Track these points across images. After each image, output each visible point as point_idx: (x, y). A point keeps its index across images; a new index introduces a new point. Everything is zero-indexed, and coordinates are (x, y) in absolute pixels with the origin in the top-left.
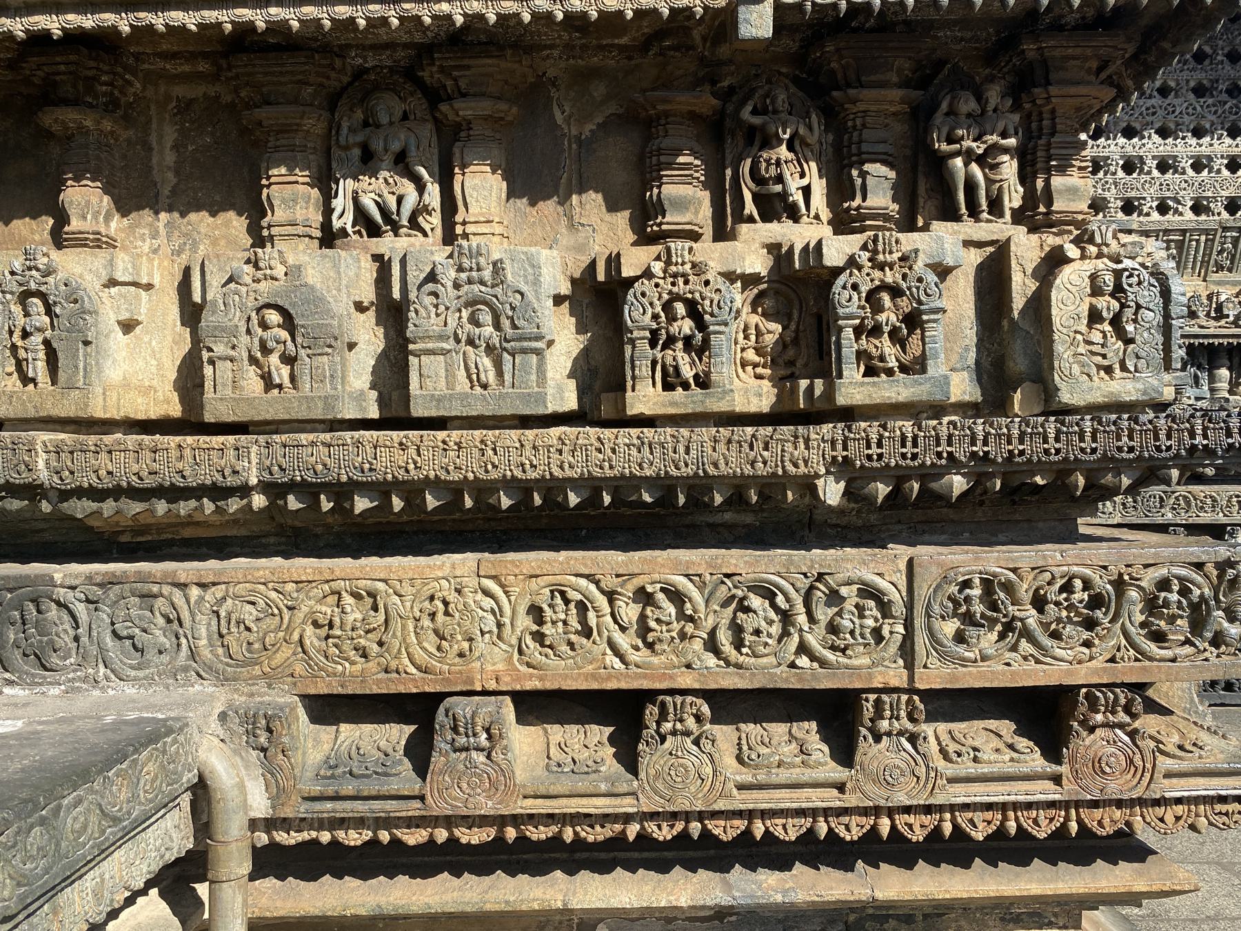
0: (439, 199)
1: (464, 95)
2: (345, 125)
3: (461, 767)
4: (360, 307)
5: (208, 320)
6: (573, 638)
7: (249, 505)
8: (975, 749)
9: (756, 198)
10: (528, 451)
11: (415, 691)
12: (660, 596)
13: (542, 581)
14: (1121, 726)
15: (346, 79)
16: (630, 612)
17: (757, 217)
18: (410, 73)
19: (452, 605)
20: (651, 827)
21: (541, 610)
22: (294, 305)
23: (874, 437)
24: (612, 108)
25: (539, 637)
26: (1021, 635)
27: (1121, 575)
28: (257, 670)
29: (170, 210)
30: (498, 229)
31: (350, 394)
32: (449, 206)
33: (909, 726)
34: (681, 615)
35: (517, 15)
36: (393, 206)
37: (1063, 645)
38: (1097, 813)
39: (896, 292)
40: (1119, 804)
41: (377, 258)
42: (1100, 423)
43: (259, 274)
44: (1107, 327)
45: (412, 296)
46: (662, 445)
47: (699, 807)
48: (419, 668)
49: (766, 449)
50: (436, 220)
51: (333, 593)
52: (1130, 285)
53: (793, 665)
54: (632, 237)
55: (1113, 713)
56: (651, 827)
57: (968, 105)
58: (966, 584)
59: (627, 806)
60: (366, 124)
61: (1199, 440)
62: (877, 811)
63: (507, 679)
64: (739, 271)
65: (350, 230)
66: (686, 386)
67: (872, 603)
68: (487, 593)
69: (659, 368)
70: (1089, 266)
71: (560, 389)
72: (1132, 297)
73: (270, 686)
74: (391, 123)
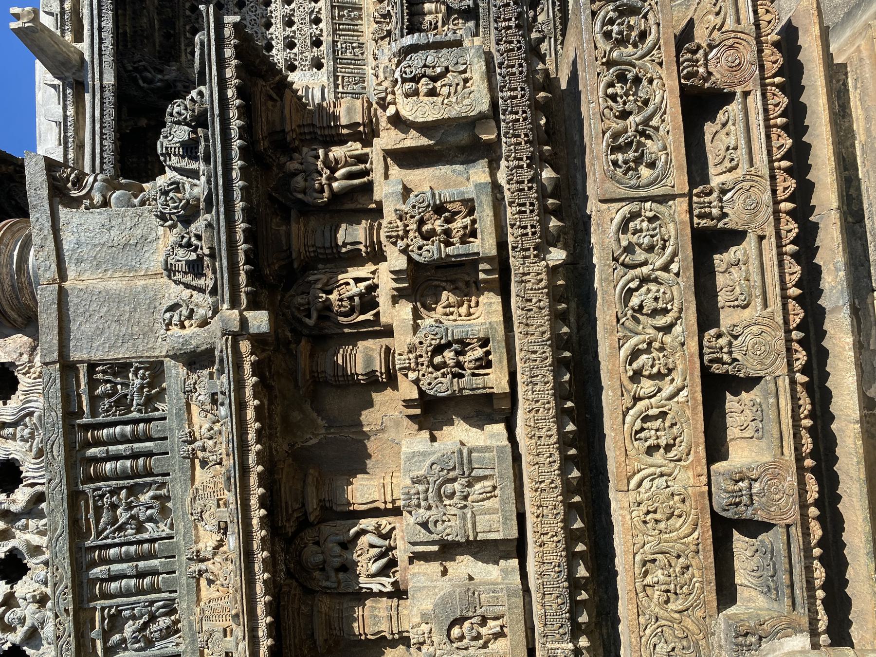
1: (303, 505)
2: (325, 584)
3: (764, 499)
4: (445, 572)
6: (667, 424)
7: (587, 648)
8: (728, 149)
9: (363, 312)
10: (541, 459)
11: (710, 532)
12: (635, 365)
14: (706, 55)
15: (295, 583)
16: (647, 386)
17: (375, 311)
18: (289, 541)
19: (650, 508)
20: (798, 365)
21: (649, 447)
22: (447, 618)
23: (521, 231)
24: (307, 407)
25: (668, 448)
26: (648, 125)
27: (603, 64)
30: (388, 480)
32: (375, 513)
33: (715, 195)
34: (648, 351)
35: (259, 474)
36: (374, 551)
37: (653, 97)
38: (768, 65)
39: (421, 222)
40: (760, 51)
41: (411, 561)
42: (504, 86)
43: (428, 641)
45: (437, 537)
46: (532, 369)
48: (694, 530)
49: (531, 300)
50: (383, 521)
51: (645, 590)
52: (411, 72)
53: (677, 274)
54: (389, 391)
55: (697, 61)
56: (798, 365)
57: (299, 181)
58: (615, 163)
59: (784, 383)
60: (323, 570)
61: (512, 24)
62: (776, 213)
63: (699, 469)
64: (412, 322)
65: (392, 580)
66: (488, 353)
67: (631, 225)
68: (640, 485)
69: (477, 372)
70: (400, 99)
71: (492, 436)
72: (419, 71)
73: (713, 634)
74: (323, 553)
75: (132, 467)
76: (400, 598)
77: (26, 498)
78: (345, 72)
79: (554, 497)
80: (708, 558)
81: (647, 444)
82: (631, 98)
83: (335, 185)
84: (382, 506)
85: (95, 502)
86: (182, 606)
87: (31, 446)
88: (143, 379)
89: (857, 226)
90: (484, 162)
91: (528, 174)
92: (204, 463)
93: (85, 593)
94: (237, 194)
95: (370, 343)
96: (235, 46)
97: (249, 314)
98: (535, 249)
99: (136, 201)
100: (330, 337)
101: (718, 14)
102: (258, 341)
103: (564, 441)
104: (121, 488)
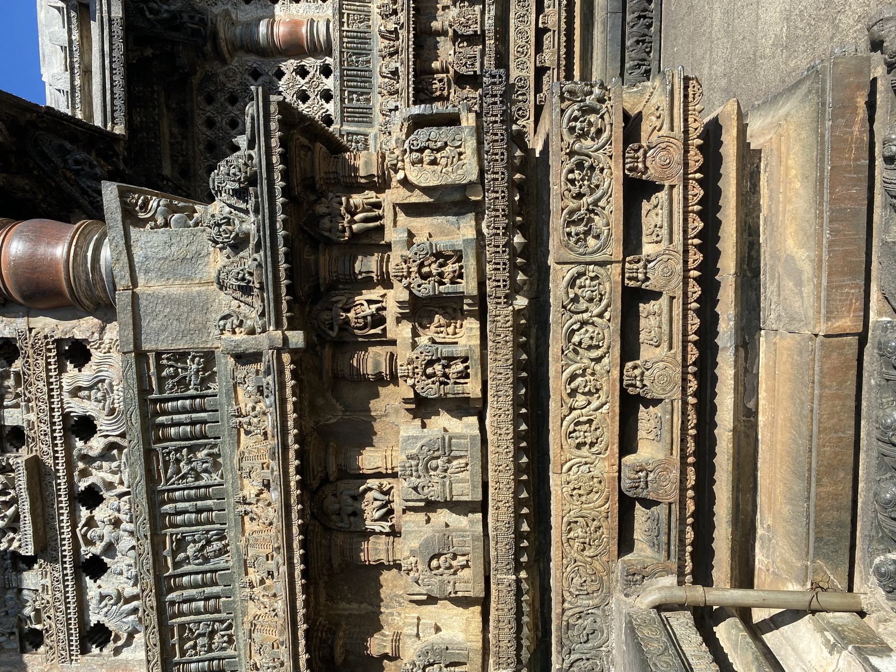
0: (374, 480)
1: (326, 468)
2: (340, 525)
4: (428, 521)
5: (436, 593)
6: (593, 428)
8: (656, 226)
9: (373, 327)
10: (500, 450)
12: (573, 385)
13: (564, 443)
14: (645, 153)
16: (581, 400)
20: (690, 391)
21: (579, 443)
23: (495, 284)
24: (329, 394)
25: (592, 445)
27: (566, 154)
28: (605, 578)
29: (380, 607)
30: (389, 453)
31: (471, 527)
32: (378, 475)
33: (642, 263)
34: (583, 375)
35: (296, 451)
36: (378, 503)
38: (691, 163)
39: (421, 265)
40: (686, 151)
41: (404, 511)
43: (414, 569)
44: (439, 155)
45: (423, 497)
46: (497, 386)
47: (680, 369)
48: (606, 502)
50: (385, 481)
53: (609, 320)
54: (391, 386)
57: (326, 222)
58: (569, 234)
59: (678, 405)
60: (339, 514)
63: (613, 460)
65: (390, 524)
66: (467, 368)
67: (578, 281)
68: (570, 469)
69: (458, 381)
70: (408, 166)
71: (468, 426)
73: (613, 572)
75: (191, 432)
76: (395, 536)
77: (102, 446)
78: (351, 10)
79: (508, 477)
80: (614, 522)
81: (577, 441)
82: (586, 182)
83: (354, 227)
84: (384, 472)
85: (164, 457)
86: (231, 534)
87: (104, 406)
88: (198, 364)
89: (754, 280)
90: (472, 215)
91: (502, 241)
92: (247, 433)
93: (158, 523)
94: (281, 241)
95: (377, 349)
96: (279, 121)
97: (289, 334)
98: (505, 298)
99: (191, 223)
100: (348, 343)
101: (659, 117)
102: (294, 352)
103: (518, 437)
104: (183, 448)
